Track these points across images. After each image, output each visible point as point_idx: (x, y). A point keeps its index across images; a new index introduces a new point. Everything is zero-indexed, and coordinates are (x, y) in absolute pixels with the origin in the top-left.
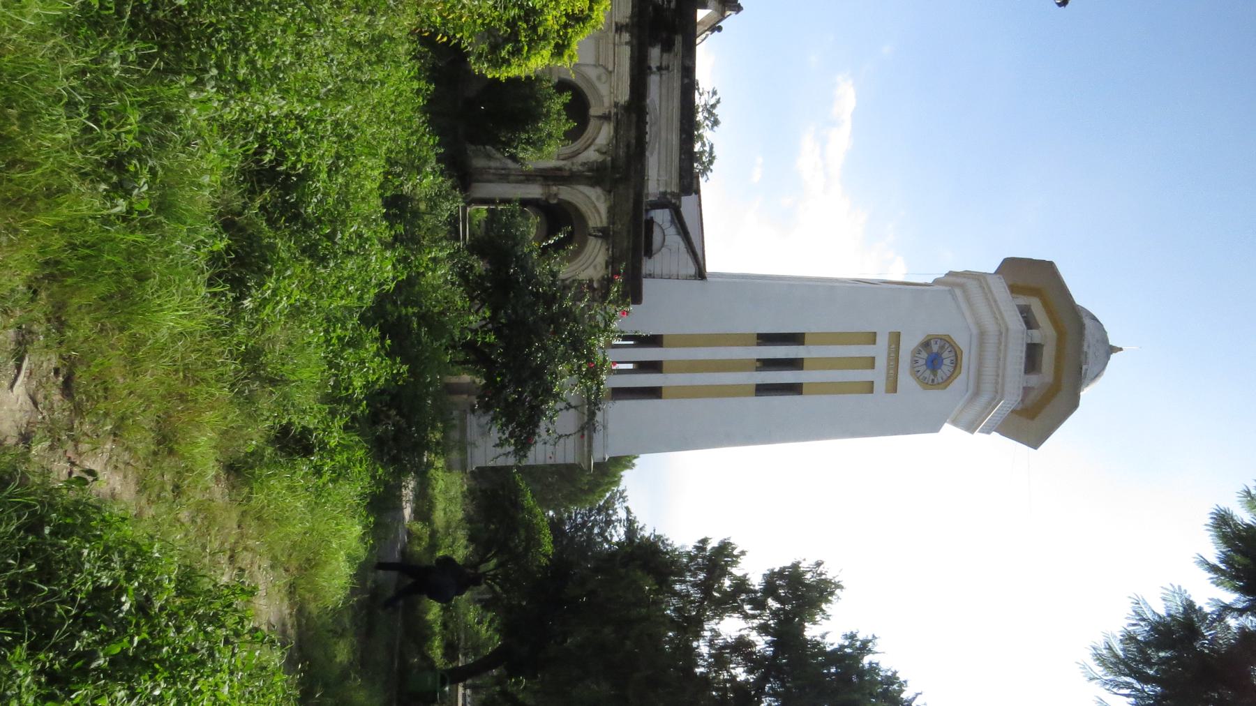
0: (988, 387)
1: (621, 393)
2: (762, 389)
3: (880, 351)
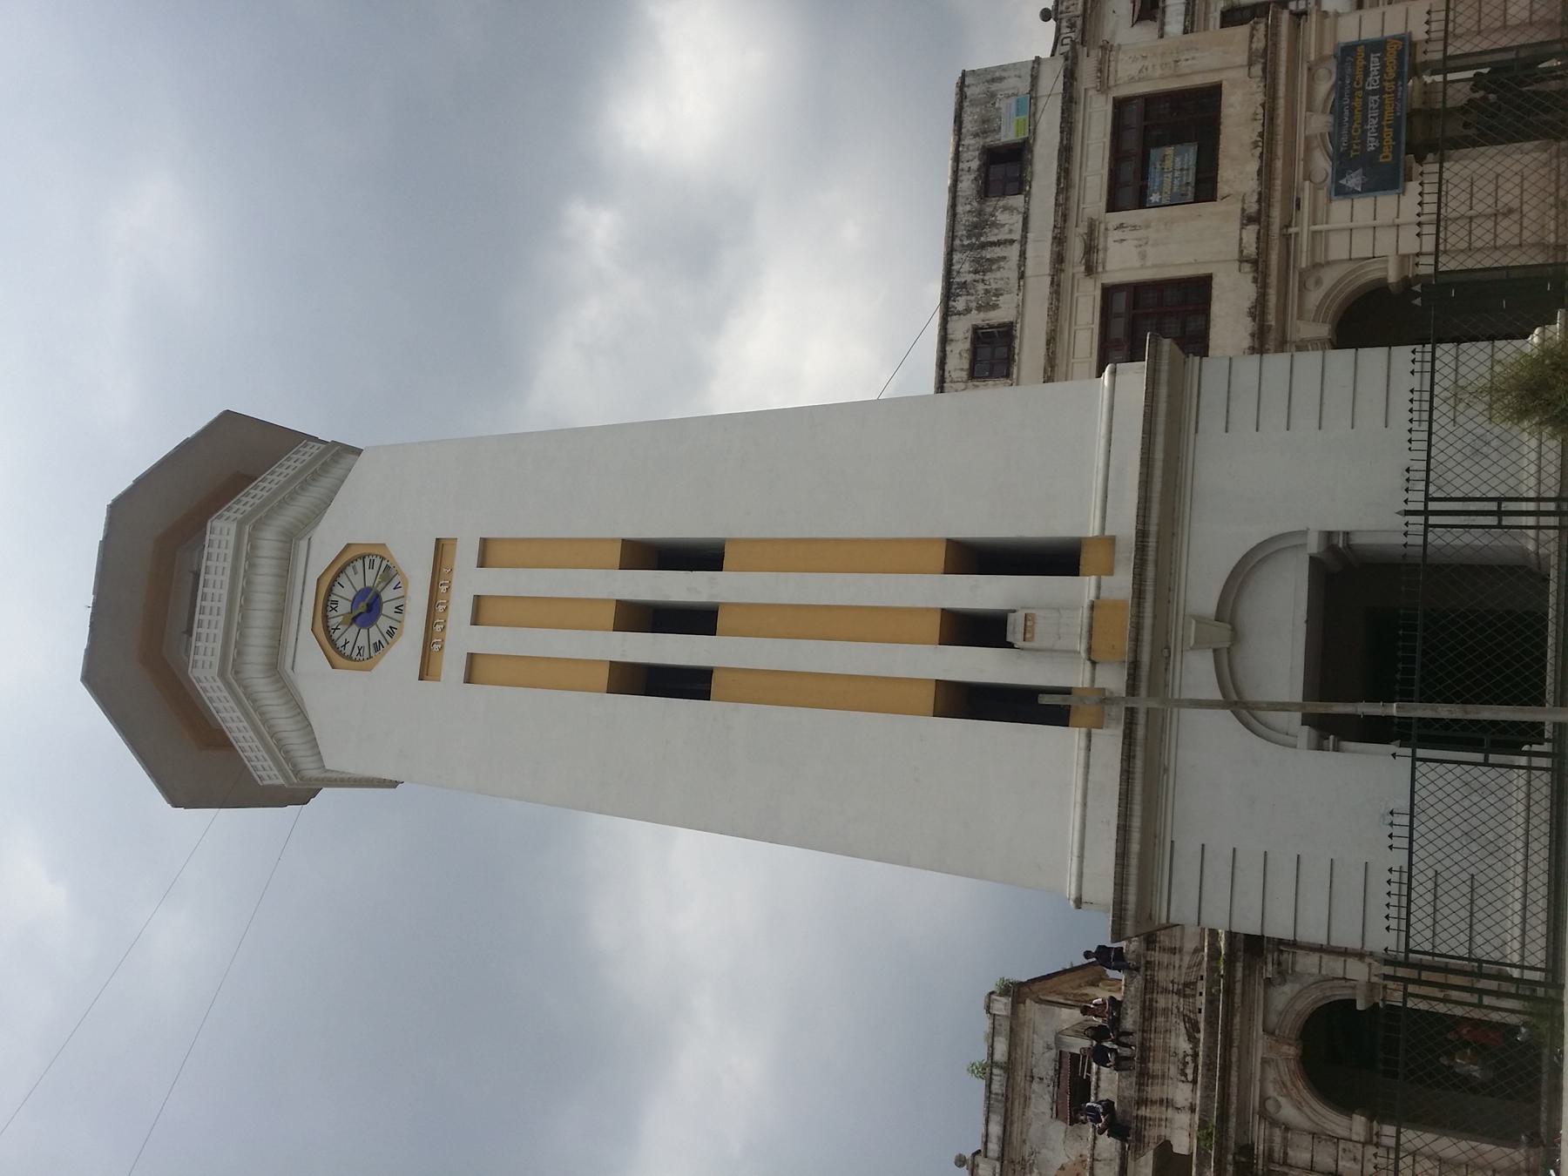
0: (269, 544)
1: (1058, 559)
2: (706, 557)
3: (461, 637)
